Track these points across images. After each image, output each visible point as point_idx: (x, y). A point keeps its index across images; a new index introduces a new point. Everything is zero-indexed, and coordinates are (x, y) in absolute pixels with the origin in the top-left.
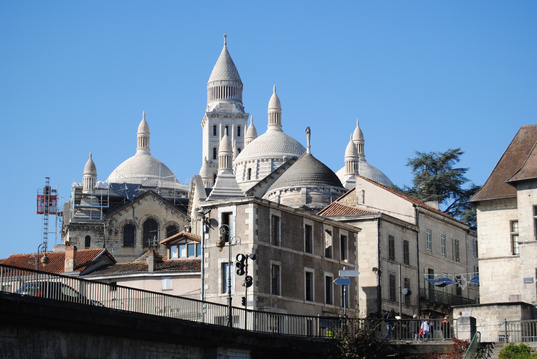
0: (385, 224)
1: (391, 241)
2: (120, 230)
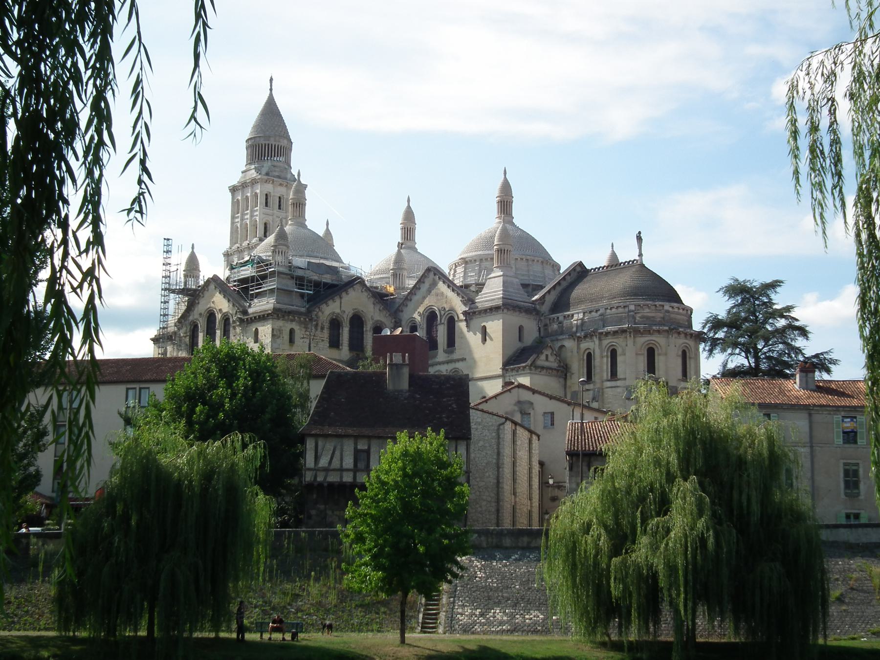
2: (327, 325)
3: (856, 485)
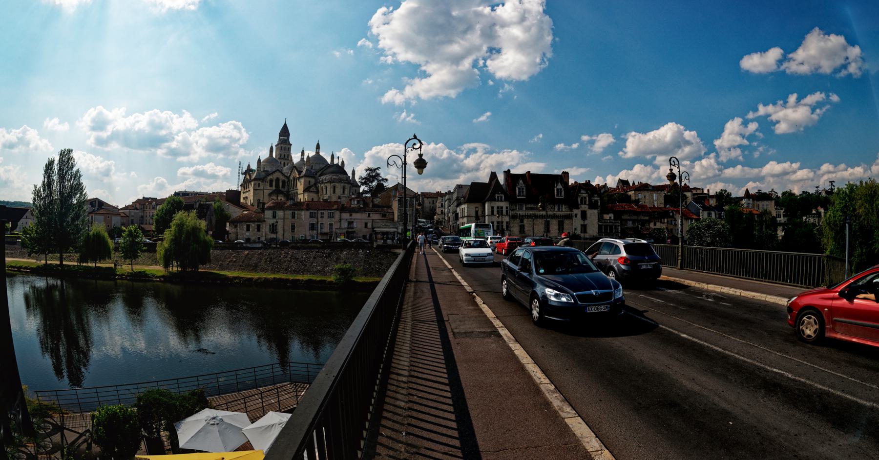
3: (294, 229)
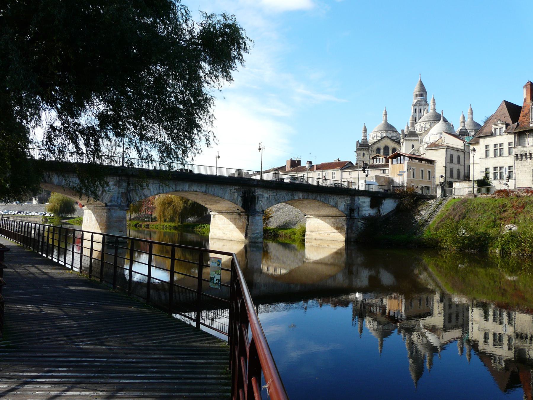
0: (448, 150)
1: (452, 156)
2: (375, 150)
